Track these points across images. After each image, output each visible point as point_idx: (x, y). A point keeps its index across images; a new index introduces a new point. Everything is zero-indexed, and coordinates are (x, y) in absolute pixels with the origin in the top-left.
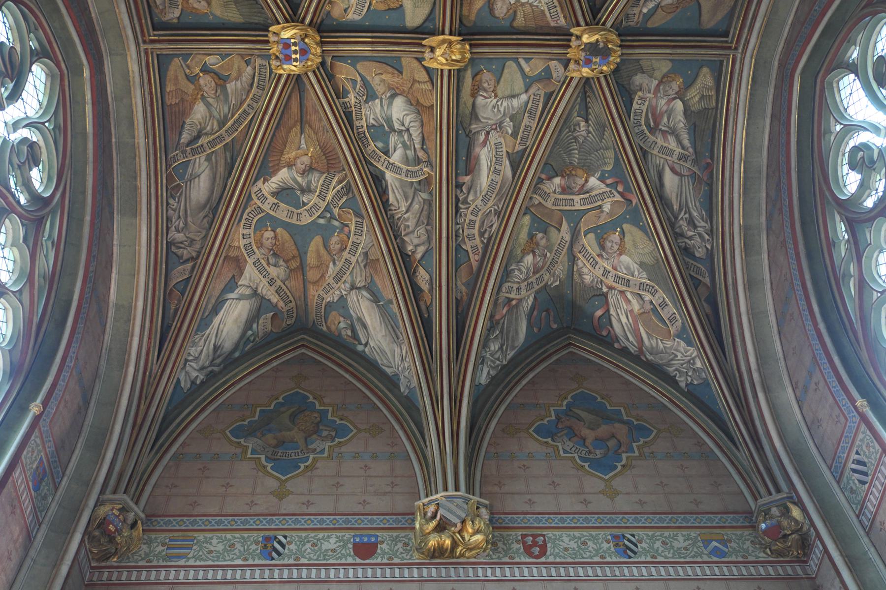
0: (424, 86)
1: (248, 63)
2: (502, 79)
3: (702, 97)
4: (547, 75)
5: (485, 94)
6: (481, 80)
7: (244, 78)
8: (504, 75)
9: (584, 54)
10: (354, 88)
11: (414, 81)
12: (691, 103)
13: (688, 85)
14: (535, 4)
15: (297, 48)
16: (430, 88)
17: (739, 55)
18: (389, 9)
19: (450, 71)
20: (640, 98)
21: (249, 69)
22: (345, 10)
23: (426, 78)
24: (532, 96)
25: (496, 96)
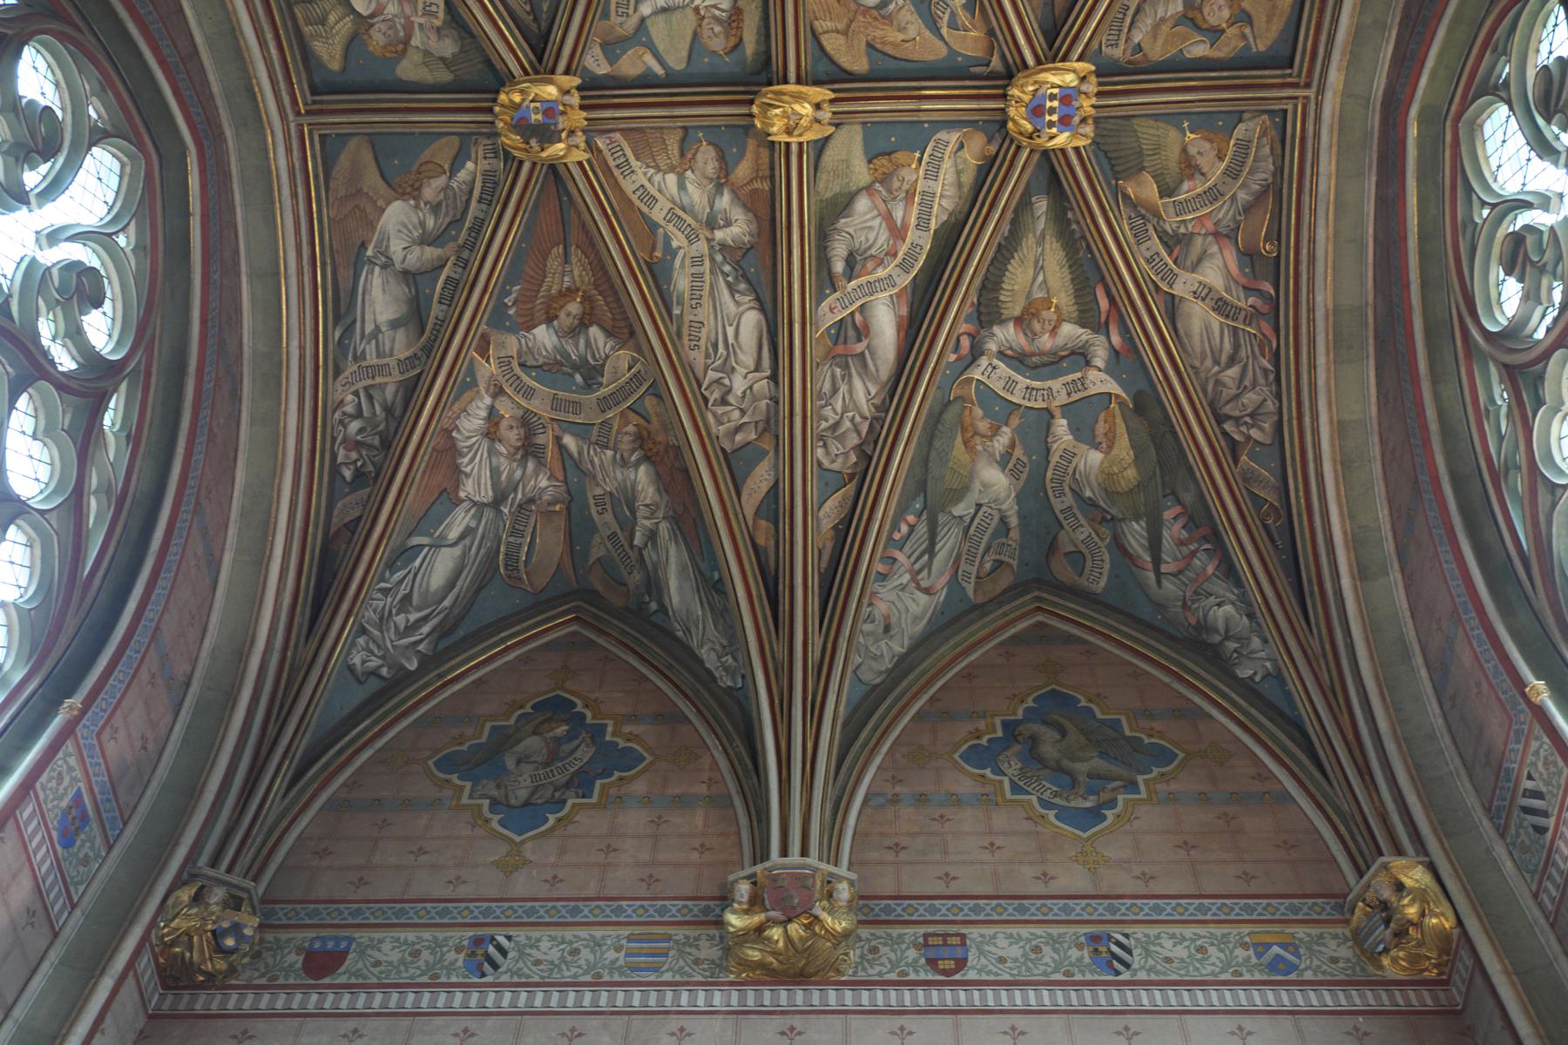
0: (829, 24)
1: (1139, 48)
2: (689, 39)
3: (323, 21)
4: (612, 48)
5: (717, 13)
6: (727, 38)
7: (1149, 21)
8: (687, 46)
9: (560, 127)
10: (953, 14)
11: (845, 32)
12: (340, 10)
13: (354, 42)
14: (652, 171)
15: (1048, 118)
16: (816, 23)
17: (291, 117)
18: (889, 154)
19: (786, 82)
20: (434, 15)
21: (1137, 37)
22: (961, 146)
23: (825, 40)
24: (631, 12)
25: (697, 10)
